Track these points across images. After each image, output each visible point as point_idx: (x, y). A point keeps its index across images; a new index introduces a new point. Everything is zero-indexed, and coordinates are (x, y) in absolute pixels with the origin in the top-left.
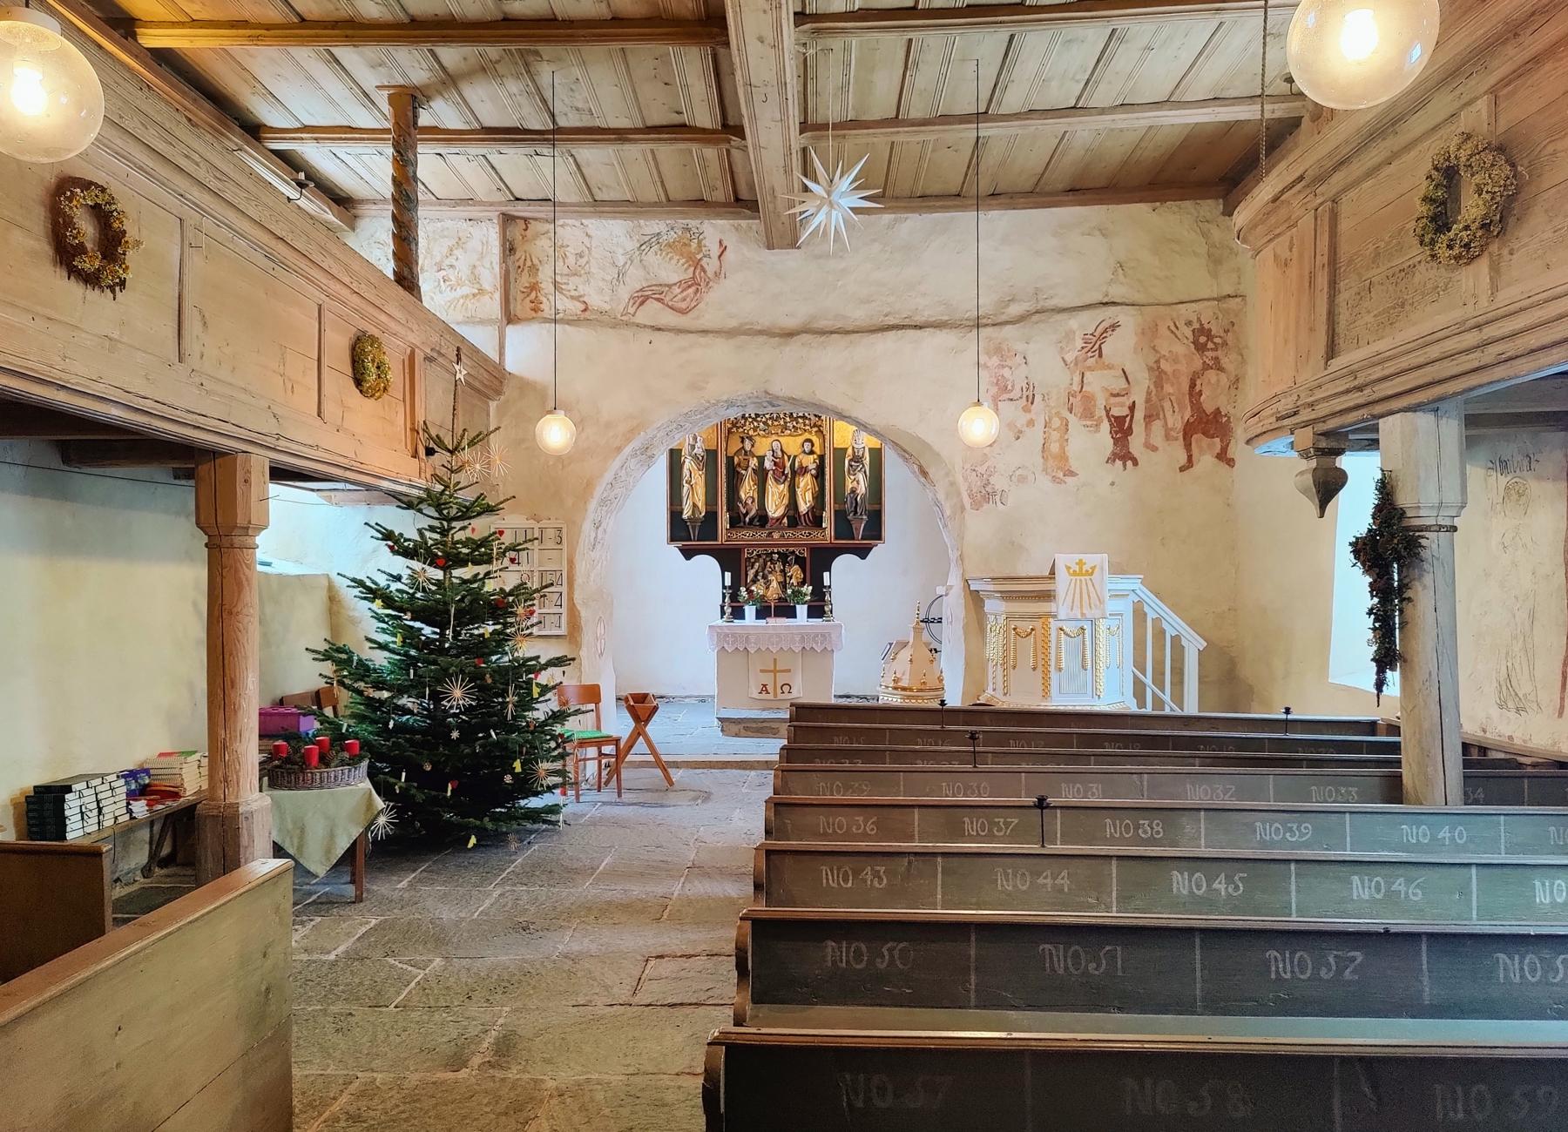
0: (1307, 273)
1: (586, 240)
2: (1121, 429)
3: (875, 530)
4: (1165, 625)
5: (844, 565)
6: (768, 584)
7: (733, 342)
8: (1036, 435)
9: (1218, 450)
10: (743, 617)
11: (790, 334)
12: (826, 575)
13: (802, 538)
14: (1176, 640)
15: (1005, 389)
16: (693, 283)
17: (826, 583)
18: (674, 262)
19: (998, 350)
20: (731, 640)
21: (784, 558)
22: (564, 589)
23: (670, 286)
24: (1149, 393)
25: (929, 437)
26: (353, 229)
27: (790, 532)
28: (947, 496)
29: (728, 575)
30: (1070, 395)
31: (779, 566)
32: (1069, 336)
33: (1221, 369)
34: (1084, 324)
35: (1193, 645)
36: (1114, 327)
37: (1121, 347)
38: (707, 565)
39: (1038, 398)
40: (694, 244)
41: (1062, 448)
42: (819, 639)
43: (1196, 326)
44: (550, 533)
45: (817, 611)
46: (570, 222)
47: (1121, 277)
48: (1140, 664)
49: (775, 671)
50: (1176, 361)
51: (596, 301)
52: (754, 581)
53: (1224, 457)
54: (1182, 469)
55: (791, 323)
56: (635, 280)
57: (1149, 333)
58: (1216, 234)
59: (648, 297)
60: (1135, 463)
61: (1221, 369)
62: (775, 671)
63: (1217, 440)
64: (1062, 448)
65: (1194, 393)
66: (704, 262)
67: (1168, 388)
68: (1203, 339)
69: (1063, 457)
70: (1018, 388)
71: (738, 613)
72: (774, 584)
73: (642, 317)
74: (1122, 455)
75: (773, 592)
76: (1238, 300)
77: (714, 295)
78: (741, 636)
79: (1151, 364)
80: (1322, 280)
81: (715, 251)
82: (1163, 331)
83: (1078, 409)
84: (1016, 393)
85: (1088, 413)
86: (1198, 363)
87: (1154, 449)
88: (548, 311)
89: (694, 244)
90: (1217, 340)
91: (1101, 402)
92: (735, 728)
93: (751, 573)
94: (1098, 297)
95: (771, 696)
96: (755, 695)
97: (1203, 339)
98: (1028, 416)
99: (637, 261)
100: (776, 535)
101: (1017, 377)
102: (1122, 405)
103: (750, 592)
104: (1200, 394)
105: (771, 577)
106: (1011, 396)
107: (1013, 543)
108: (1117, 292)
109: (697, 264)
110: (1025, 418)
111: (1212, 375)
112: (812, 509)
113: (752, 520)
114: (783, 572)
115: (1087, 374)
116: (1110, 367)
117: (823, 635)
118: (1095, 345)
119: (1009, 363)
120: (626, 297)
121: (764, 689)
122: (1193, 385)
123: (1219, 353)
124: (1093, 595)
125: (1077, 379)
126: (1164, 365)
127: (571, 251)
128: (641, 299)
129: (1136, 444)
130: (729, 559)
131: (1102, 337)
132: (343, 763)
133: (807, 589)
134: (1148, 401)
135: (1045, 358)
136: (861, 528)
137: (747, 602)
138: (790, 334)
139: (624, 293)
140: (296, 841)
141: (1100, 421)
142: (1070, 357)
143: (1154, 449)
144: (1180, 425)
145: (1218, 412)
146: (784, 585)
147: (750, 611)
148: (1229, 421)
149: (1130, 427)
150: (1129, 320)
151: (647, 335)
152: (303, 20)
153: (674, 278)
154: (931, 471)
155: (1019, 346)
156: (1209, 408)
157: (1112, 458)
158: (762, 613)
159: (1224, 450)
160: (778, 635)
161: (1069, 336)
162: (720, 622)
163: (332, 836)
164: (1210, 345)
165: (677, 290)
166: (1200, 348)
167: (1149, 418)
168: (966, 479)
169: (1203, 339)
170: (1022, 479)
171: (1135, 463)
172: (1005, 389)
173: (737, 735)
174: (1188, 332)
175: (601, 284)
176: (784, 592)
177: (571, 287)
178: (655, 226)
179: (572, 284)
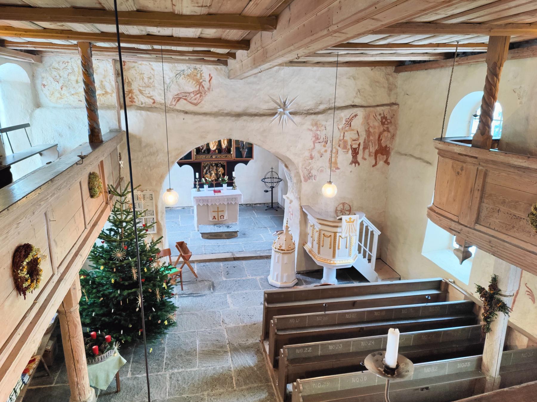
0: (470, 187)
1: (152, 71)
2: (355, 152)
3: (250, 155)
4: (369, 228)
7: (216, 119)
8: (327, 155)
9: (385, 160)
11: (239, 115)
13: (223, 158)
14: (372, 232)
15: (318, 139)
16: (199, 92)
17: (233, 176)
18: (190, 83)
19: (316, 124)
20: (201, 201)
21: (217, 165)
22: (155, 217)
23: (189, 93)
24: (365, 140)
25: (291, 157)
26: (41, 62)
27: (219, 156)
28: (295, 176)
29: (197, 174)
30: (340, 140)
31: (215, 168)
32: (341, 119)
33: (389, 131)
34: (345, 114)
35: (377, 233)
36: (356, 116)
37: (358, 123)
38: (188, 169)
39: (329, 142)
40: (199, 75)
41: (336, 160)
43: (382, 115)
44: (148, 195)
45: (231, 184)
46: (144, 63)
47: (359, 96)
48: (360, 240)
49: (218, 211)
50: (375, 128)
51: (159, 99)
52: (206, 173)
53: (387, 162)
54: (373, 166)
55: (239, 110)
56: (174, 91)
57: (367, 118)
58: (391, 79)
59: (180, 98)
60: (359, 164)
61: (389, 131)
62: (218, 211)
63: (385, 156)
64: (336, 160)
65: (379, 140)
66: (203, 83)
67: (371, 138)
68: (384, 120)
69: (336, 163)
70: (322, 138)
73: (178, 107)
74: (355, 161)
76: (397, 106)
77: (208, 98)
78: (205, 200)
79: (367, 129)
80: (477, 194)
81: (208, 79)
82: (372, 117)
83: (342, 146)
84: (321, 140)
85: (345, 147)
86: (382, 129)
87: (365, 159)
88: (137, 103)
89: (199, 75)
90: (389, 121)
91: (349, 143)
92: (206, 236)
93: (205, 171)
94: (350, 103)
96: (211, 219)
97: (384, 120)
98: (325, 148)
99: (175, 81)
100: (214, 157)
101: (322, 134)
102: (356, 144)
103: (206, 180)
104: (381, 140)
106: (319, 141)
107: (317, 193)
108: (358, 101)
109: (200, 84)
110: (323, 149)
111: (386, 134)
112: (227, 147)
113: (204, 151)
114: (217, 170)
115: (346, 133)
116: (353, 130)
117: (235, 198)
118: (349, 123)
119: (320, 129)
120: (171, 97)
121: (214, 218)
122: (379, 137)
123: (389, 126)
124: (353, 229)
125: (342, 135)
126: (371, 130)
127: (145, 76)
128: (178, 99)
129: (359, 158)
130: (197, 167)
131: (351, 120)
132: (108, 350)
133: (226, 178)
134: (364, 142)
135: (331, 126)
136: (245, 152)
137: (205, 184)
138: (239, 115)
139: (170, 96)
140: (95, 382)
141: (349, 149)
142: (340, 127)
143: (365, 159)
144: (374, 151)
145: (386, 146)
146: (217, 174)
147: (206, 186)
148: (389, 150)
149: (358, 152)
150: (360, 112)
151: (182, 116)
152: (45, 28)
153: (191, 90)
154: (290, 167)
155: (324, 123)
156: (384, 145)
157: (351, 164)
159: (387, 159)
160: (219, 199)
161: (341, 119)
162: (195, 193)
163: (108, 376)
164: (386, 123)
165: (192, 95)
166: (383, 123)
167: (364, 149)
168: (303, 171)
169: (384, 120)
170: (322, 171)
171: (359, 164)
172: (318, 139)
173: (207, 238)
174: (379, 117)
175: (160, 91)
177: (147, 92)
178: (182, 67)
179: (147, 91)
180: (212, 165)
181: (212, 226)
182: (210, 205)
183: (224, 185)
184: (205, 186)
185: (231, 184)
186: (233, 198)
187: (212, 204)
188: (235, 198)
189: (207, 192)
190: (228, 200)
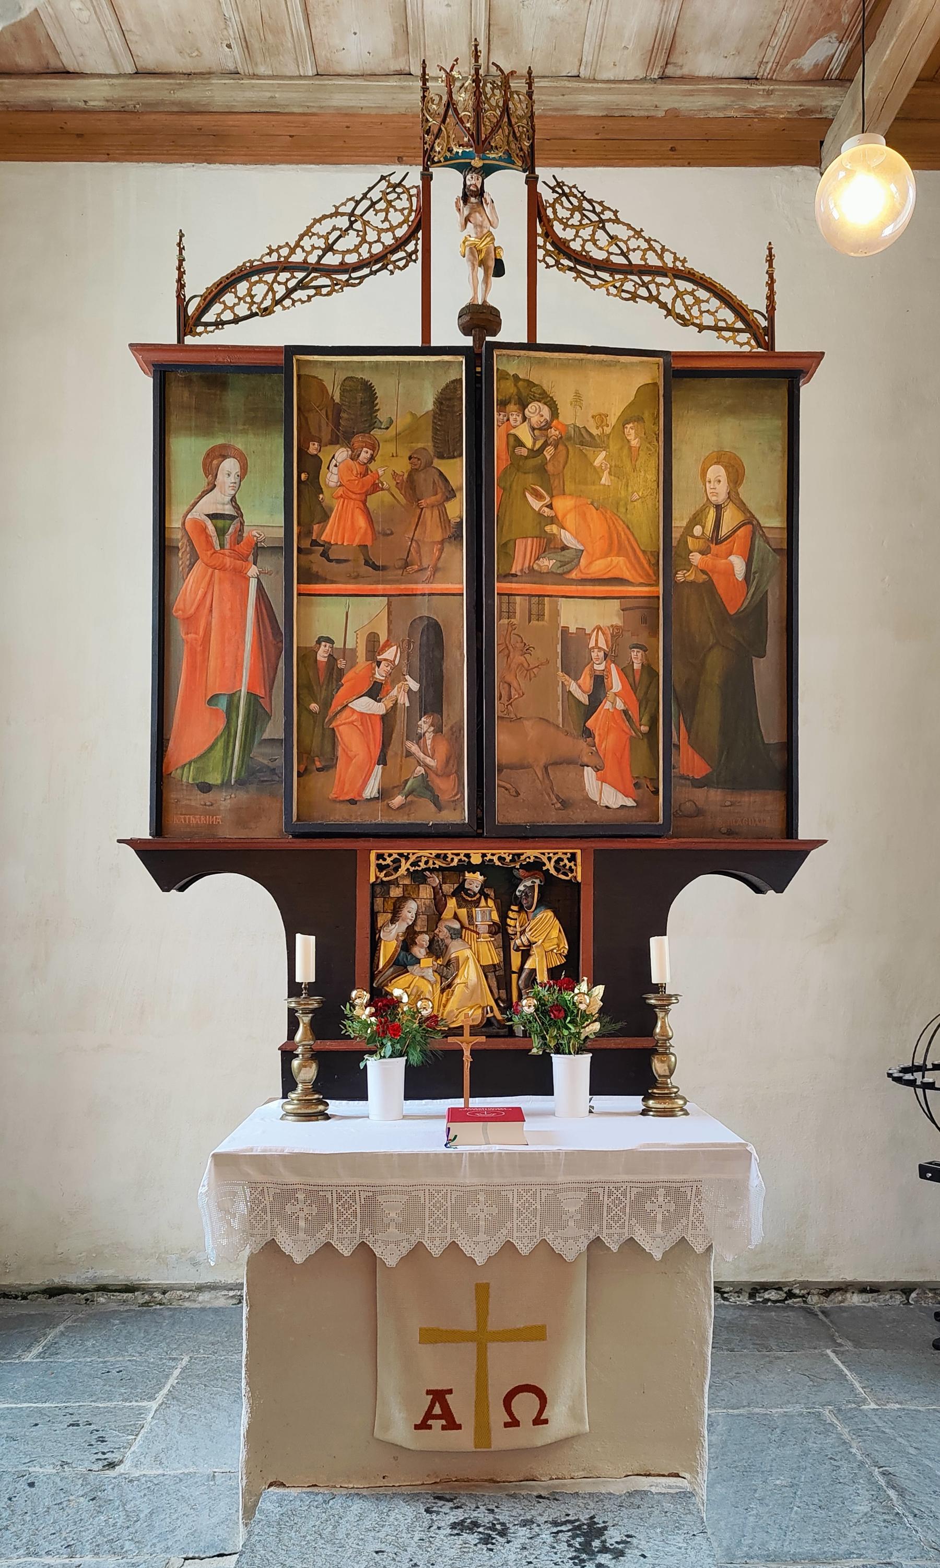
5: (707, 905)
6: (447, 974)
10: (359, 1092)
12: (653, 941)
20: (302, 1210)
21: (501, 883)
29: (306, 944)
31: (486, 913)
42: (659, 1207)
45: (630, 1068)
62: (481, 1338)
71: (340, 1078)
72: (470, 974)
75: (466, 999)
95: (463, 1439)
96: (399, 1425)
103: (382, 1002)
105: (457, 950)
114: (500, 930)
117: (676, 1193)
121: (438, 1409)
133: (589, 996)
146: (500, 976)
147: (384, 1073)
158: (418, 1085)
162: (271, 1127)
176: (508, 1005)
180: (460, 892)
181: (404, 1514)
182: (390, 1256)
183: (556, 1059)
184: (372, 1065)
185: (630, 1068)
186: (647, 1193)
187: (418, 1250)
188: (675, 1187)
189: (386, 1120)
190: (593, 1207)
